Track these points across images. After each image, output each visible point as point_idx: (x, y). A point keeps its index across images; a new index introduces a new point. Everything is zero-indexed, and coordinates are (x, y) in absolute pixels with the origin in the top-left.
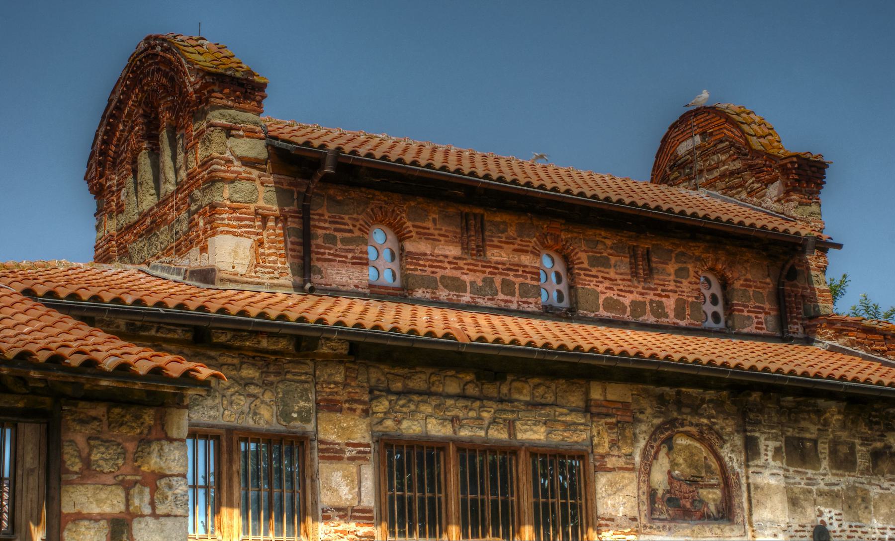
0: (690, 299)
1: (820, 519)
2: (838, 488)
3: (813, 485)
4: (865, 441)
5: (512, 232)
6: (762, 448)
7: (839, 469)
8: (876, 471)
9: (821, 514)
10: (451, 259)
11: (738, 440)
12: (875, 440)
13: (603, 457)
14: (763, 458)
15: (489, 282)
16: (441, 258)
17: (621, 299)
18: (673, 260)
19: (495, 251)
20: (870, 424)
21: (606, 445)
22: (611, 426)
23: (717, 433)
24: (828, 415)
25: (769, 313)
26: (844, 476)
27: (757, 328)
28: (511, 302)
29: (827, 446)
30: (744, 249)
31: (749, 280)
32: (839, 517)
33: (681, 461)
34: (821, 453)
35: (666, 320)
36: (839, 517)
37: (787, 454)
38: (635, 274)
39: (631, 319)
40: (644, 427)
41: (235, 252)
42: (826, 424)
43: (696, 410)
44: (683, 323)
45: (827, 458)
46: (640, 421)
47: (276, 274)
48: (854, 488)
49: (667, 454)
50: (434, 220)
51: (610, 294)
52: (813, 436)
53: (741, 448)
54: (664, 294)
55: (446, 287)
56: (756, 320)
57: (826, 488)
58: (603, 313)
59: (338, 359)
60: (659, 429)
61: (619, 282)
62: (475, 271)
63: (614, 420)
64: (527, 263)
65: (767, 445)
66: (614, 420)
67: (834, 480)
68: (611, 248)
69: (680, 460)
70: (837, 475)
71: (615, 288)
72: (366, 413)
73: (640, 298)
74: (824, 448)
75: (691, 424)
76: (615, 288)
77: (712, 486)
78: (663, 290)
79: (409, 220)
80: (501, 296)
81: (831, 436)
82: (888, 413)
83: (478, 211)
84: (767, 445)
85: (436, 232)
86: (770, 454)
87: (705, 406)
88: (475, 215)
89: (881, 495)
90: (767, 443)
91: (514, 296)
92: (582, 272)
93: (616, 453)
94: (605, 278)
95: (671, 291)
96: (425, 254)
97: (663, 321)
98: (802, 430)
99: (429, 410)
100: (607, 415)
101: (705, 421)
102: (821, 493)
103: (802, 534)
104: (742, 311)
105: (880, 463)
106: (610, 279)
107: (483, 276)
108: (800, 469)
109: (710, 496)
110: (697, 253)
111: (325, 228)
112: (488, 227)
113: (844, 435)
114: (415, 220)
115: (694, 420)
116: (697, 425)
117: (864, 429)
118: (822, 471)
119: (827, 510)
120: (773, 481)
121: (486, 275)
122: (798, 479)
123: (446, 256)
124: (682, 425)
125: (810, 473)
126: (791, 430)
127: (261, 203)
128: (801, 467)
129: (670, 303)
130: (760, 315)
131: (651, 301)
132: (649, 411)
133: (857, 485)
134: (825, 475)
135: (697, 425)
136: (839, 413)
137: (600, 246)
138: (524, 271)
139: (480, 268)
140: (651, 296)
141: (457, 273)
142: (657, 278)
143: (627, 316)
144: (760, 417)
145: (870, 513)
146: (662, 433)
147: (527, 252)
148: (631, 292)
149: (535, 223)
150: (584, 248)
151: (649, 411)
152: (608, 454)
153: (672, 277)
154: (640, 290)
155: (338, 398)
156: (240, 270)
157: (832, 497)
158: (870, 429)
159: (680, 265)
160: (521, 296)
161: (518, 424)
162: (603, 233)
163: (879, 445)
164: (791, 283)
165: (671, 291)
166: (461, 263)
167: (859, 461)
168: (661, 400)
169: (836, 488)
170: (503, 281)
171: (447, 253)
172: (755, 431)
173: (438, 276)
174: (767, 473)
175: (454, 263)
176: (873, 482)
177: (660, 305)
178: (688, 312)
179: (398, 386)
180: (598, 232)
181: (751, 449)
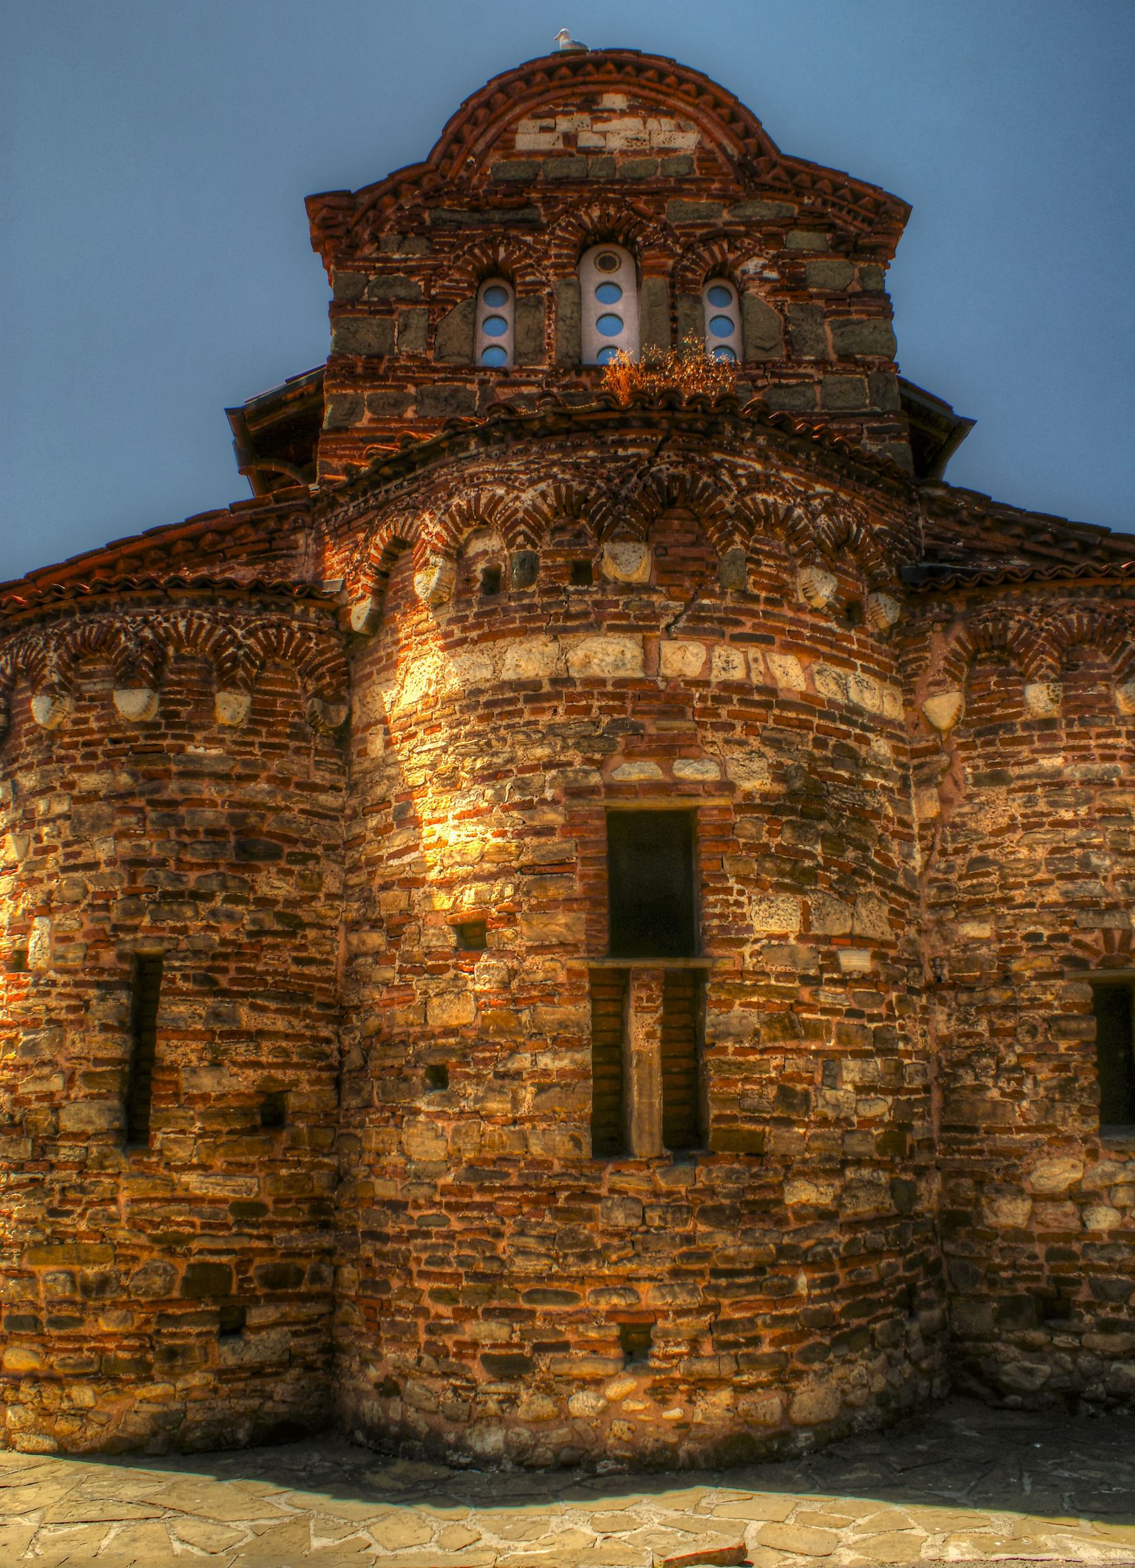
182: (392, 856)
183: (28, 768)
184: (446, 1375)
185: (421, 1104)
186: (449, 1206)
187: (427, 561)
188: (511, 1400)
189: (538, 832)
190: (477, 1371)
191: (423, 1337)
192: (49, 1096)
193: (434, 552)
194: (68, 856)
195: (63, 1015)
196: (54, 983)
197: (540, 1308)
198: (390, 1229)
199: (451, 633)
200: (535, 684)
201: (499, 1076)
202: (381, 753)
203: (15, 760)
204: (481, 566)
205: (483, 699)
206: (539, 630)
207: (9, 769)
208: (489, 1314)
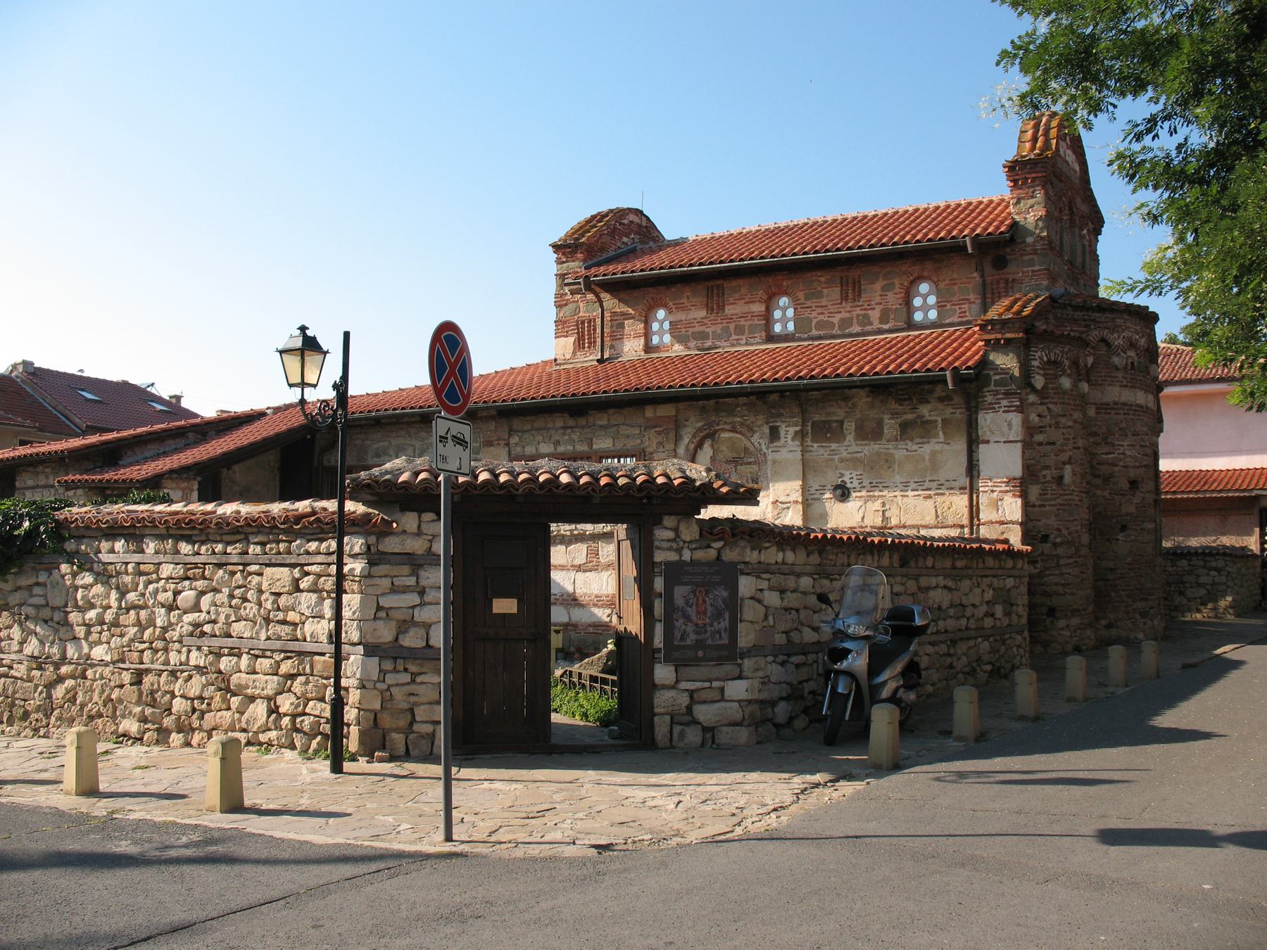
0: (894, 307)
1: (841, 479)
2: (862, 454)
3: (836, 454)
4: (895, 414)
5: (743, 291)
6: (782, 433)
7: (864, 440)
8: (904, 437)
9: (842, 475)
10: (699, 320)
11: (766, 430)
12: (906, 413)
13: (652, 453)
14: (783, 440)
15: (726, 330)
16: (692, 321)
17: (831, 319)
18: (881, 279)
19: (731, 307)
20: (900, 401)
21: (654, 445)
22: (659, 433)
23: (748, 426)
24: (856, 400)
25: (974, 302)
26: (870, 445)
27: (959, 317)
28: (742, 339)
29: (853, 424)
30: (952, 255)
31: (955, 279)
32: (860, 477)
33: (725, 448)
34: (847, 430)
35: (870, 327)
36: (860, 477)
37: (812, 434)
38: (844, 297)
39: (839, 332)
40: (688, 430)
41: (565, 347)
42: (854, 406)
43: (731, 412)
44: (886, 327)
45: (853, 433)
46: (685, 426)
47: (588, 354)
48: (878, 453)
49: (712, 446)
50: (688, 297)
51: (821, 317)
52: (839, 418)
53: (768, 435)
54: (869, 307)
55: (694, 339)
56: (959, 311)
57: (849, 456)
58: (814, 332)
59: (492, 418)
60: (700, 430)
61: (830, 307)
62: (716, 324)
63: (661, 429)
64: (755, 310)
65: (788, 431)
66: (661, 429)
67: (858, 449)
68: (825, 283)
69: (723, 448)
70: (862, 445)
71: (826, 312)
72: (508, 444)
73: (848, 315)
74: (850, 426)
75: (725, 423)
76: (826, 312)
77: (749, 463)
78: (869, 305)
79: (671, 300)
80: (734, 337)
81: (859, 416)
82: (923, 389)
83: (718, 282)
84: (788, 431)
85: (689, 305)
86: (790, 437)
87: (739, 409)
88: (718, 286)
89: (907, 457)
90: (787, 429)
91: (743, 334)
92: (798, 307)
93: (662, 450)
94: (818, 307)
95: (877, 304)
96: (682, 321)
97: (869, 328)
98: (829, 414)
99: (540, 438)
100: (655, 427)
101: (739, 419)
102: (842, 460)
103: (822, 492)
104: (946, 306)
105: (909, 430)
106: (822, 307)
107: (722, 325)
108: (824, 444)
109: (748, 470)
110: (904, 269)
111: (616, 320)
112: (727, 291)
113: (872, 414)
114: (675, 300)
115: (729, 420)
116: (730, 423)
117: (894, 405)
118: (845, 443)
119: (848, 473)
120: (790, 456)
121: (725, 325)
122: (822, 451)
123: (695, 319)
124: (718, 425)
125: (834, 446)
126: (818, 416)
127: (581, 314)
128: (825, 442)
129: (875, 315)
130: (963, 306)
131: (858, 316)
132: (693, 419)
133: (882, 450)
134: (849, 446)
135: (730, 423)
136: (867, 396)
137: (816, 284)
138: (752, 316)
139: (719, 321)
140: (858, 311)
141: (702, 329)
142: (864, 297)
143: (836, 331)
144: (782, 411)
145: (894, 471)
146: (702, 432)
147: (754, 302)
148: (840, 312)
149: (762, 280)
150: (801, 288)
151: (693, 419)
152: (656, 451)
153: (880, 292)
154: (849, 309)
155: (491, 439)
156: (568, 356)
157: (854, 462)
158: (901, 405)
159: (886, 282)
160: (750, 333)
161: (594, 439)
162: (819, 273)
163: (910, 417)
164: (1001, 272)
165: (877, 304)
166: (705, 321)
167: (886, 431)
168: (703, 410)
169: (858, 455)
170: (736, 326)
171: (696, 316)
172: (776, 422)
173: (690, 333)
174: (784, 451)
175: (701, 323)
176: (899, 446)
177: (866, 317)
178: (892, 316)
179: (528, 427)
180: (814, 273)
181: (774, 435)
182: (1102, 454)
183: (1056, 403)
184: (1130, 619)
185: (1119, 537)
186: (1129, 569)
187: (1119, 354)
188: (1145, 623)
189: (1147, 455)
190: (1137, 616)
191: (1123, 609)
192: (1077, 532)
193: (1122, 350)
194: (1075, 443)
195: (1077, 502)
196: (1073, 491)
197: (1150, 597)
198: (1109, 577)
199: (1122, 382)
200: (1142, 407)
201: (1141, 529)
202: (1094, 416)
203: (1048, 398)
204: (1130, 361)
205: (1133, 408)
206: (1142, 389)
207: (1044, 401)
208: (1141, 599)
